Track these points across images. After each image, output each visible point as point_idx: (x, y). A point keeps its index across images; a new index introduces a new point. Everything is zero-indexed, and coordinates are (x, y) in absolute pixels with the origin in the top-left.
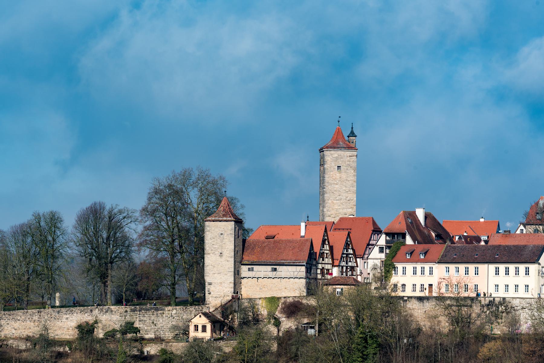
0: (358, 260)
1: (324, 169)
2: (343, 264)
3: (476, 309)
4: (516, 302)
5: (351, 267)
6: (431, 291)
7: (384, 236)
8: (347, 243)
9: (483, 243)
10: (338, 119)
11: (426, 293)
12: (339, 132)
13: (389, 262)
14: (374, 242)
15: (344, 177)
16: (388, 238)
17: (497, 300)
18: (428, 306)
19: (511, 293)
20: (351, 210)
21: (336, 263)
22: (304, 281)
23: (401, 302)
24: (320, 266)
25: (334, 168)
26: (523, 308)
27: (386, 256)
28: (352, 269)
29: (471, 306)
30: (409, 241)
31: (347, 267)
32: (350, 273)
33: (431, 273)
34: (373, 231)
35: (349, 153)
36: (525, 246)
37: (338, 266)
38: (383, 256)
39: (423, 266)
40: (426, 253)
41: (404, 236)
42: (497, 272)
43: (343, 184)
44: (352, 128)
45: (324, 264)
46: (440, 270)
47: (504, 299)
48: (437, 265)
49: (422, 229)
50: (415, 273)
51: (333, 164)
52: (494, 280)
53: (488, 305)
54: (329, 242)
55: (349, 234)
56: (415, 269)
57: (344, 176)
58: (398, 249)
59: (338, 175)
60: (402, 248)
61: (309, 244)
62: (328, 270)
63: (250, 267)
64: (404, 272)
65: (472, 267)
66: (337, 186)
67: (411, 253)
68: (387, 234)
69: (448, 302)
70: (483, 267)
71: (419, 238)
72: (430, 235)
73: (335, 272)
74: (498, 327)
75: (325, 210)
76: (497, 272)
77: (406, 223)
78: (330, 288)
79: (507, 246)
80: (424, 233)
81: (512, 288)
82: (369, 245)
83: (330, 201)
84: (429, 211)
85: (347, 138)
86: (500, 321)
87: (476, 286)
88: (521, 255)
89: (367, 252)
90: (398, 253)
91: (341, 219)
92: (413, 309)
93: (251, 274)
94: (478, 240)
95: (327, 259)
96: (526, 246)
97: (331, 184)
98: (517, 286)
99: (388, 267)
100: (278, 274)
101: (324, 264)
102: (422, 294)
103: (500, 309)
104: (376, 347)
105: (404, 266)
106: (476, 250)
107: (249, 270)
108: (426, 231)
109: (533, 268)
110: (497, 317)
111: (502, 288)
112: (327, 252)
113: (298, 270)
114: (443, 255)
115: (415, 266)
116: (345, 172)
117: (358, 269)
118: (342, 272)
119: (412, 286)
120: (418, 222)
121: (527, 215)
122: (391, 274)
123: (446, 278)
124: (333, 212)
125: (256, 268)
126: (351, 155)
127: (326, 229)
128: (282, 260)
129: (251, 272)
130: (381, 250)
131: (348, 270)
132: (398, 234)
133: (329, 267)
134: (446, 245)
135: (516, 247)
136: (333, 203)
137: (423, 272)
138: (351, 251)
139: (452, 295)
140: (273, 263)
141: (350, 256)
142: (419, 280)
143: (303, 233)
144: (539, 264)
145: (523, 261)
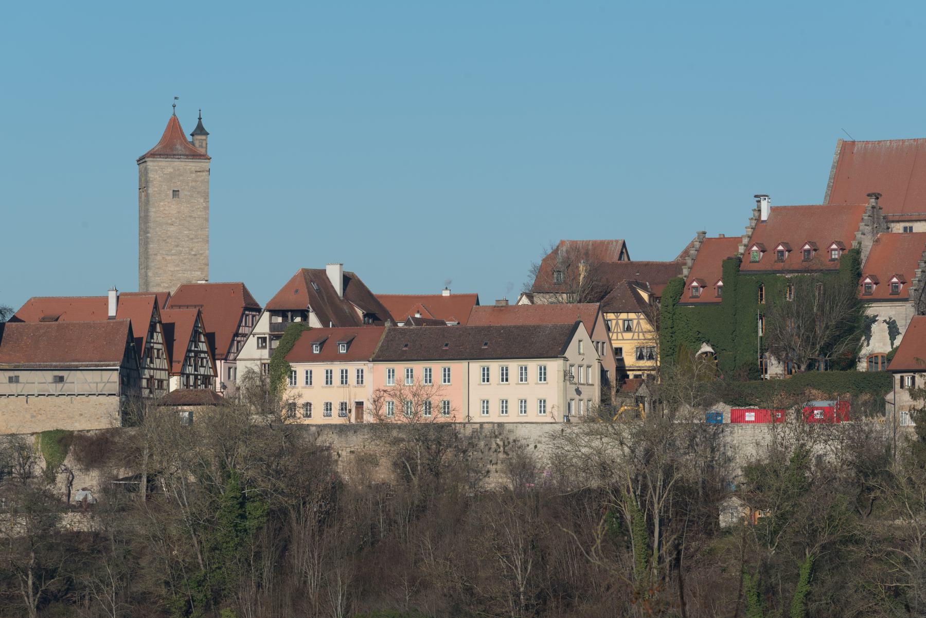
1: (147, 195)
2: (190, 370)
4: (522, 432)
5: (204, 376)
6: (360, 414)
7: (266, 315)
12: (174, 126)
19: (513, 415)
20: (199, 273)
21: (177, 367)
22: (115, 400)
24: (147, 374)
25: (167, 195)
28: (207, 380)
31: (196, 377)
34: (246, 309)
35: (193, 165)
36: (536, 328)
37: (182, 374)
40: (349, 344)
41: (304, 315)
42: (486, 378)
44: (200, 119)
45: (154, 369)
47: (501, 425)
48: (371, 365)
50: (329, 380)
52: (479, 392)
61: (126, 331)
62: (161, 381)
63: (12, 374)
64: (309, 381)
65: (438, 367)
66: (172, 229)
68: (274, 312)
69: (395, 433)
70: (458, 368)
73: (174, 383)
75: (150, 274)
76: (486, 378)
77: (309, 292)
79: (503, 328)
81: (514, 407)
82: (237, 338)
83: (159, 257)
84: (348, 269)
85: (190, 139)
87: (447, 404)
89: (234, 349)
93: (14, 388)
95: (158, 360)
96: (538, 327)
99: (278, 369)
100: (66, 387)
101: (154, 369)
107: (11, 380)
109: (554, 366)
111: (495, 407)
112: (159, 346)
113: (105, 380)
114: (382, 346)
117: (218, 380)
118: (187, 385)
119: (323, 407)
125: (23, 376)
126: (198, 169)
128: (74, 361)
129: (13, 385)
131: (199, 382)
137: (344, 380)
140: (55, 366)
141: (202, 355)
142: (337, 395)
143: (112, 312)
144: (566, 359)
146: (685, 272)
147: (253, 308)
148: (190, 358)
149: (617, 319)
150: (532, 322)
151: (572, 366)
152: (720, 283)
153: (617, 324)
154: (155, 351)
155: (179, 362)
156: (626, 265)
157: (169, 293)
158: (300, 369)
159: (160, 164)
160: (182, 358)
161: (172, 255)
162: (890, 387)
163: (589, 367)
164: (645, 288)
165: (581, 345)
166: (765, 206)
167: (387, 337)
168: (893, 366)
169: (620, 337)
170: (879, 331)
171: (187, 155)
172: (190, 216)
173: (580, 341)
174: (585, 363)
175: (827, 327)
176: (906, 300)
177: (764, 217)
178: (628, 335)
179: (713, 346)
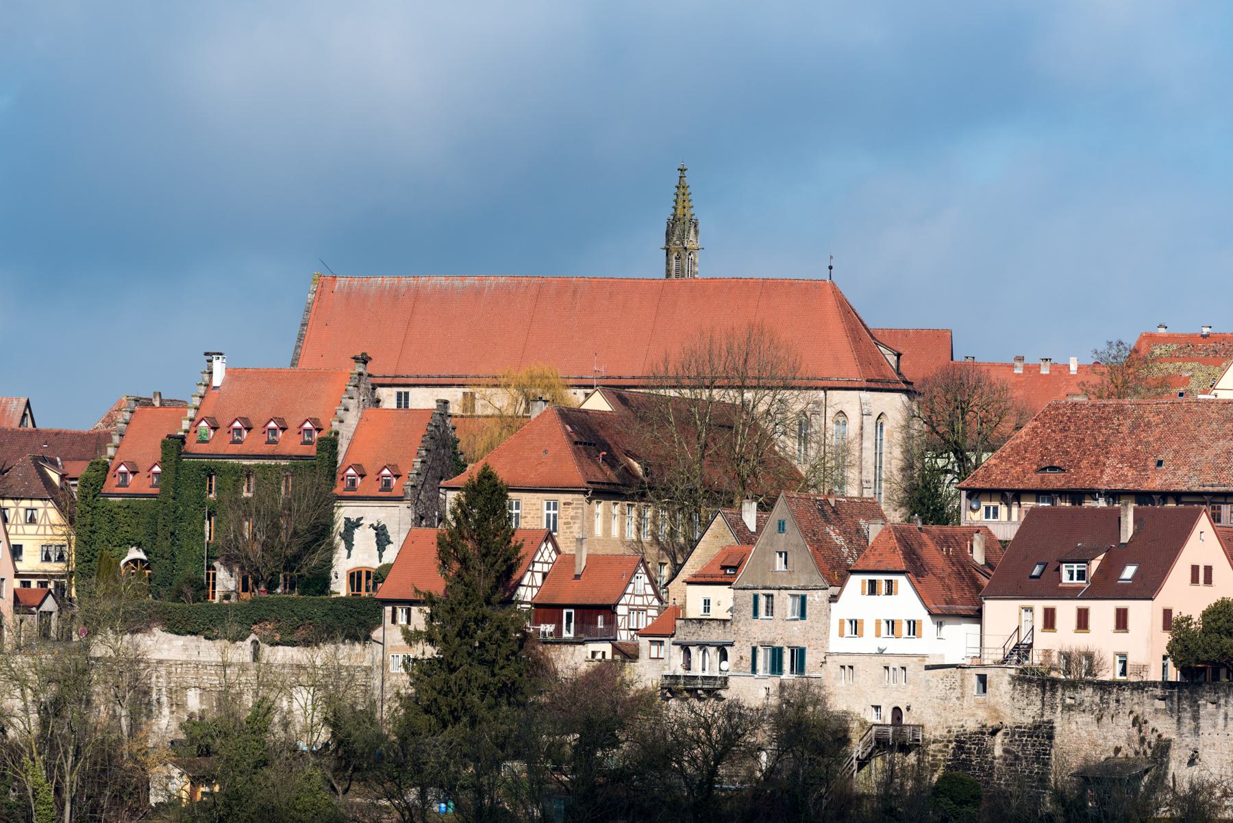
146: (111, 451)
149: (17, 507)
152: (157, 469)
153: (17, 513)
156: (30, 433)
162: (380, 623)
164: (54, 463)
166: (219, 367)
168: (384, 591)
170: (364, 537)
175: (295, 533)
176: (400, 499)
177: (217, 381)
178: (31, 529)
179: (146, 553)
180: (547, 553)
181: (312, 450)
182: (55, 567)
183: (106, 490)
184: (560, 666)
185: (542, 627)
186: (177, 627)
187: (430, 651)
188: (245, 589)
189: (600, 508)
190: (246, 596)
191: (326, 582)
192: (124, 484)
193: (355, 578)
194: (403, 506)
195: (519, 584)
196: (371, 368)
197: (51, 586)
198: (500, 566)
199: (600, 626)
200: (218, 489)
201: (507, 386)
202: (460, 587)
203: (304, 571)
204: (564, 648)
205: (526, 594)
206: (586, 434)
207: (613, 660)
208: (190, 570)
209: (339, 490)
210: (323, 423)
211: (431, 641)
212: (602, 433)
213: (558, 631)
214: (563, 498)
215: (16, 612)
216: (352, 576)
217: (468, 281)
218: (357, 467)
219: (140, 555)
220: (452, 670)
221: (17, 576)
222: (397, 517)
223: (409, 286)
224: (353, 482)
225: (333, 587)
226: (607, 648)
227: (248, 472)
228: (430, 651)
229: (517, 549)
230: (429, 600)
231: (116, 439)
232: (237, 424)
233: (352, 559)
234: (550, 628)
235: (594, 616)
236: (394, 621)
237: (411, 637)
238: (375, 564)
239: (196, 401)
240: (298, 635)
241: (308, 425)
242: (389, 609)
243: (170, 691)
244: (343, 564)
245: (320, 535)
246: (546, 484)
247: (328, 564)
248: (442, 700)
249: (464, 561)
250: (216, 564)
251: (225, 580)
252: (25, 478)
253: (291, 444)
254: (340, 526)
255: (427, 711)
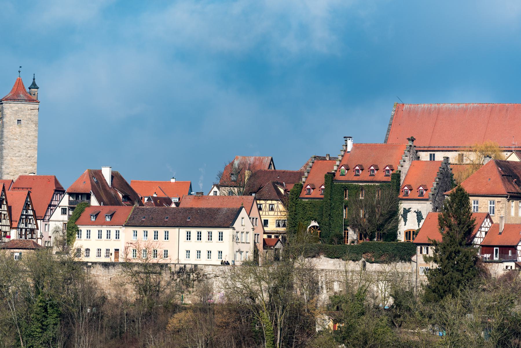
0: (39, 221)
3: (166, 276)
4: (208, 270)
5: (31, 229)
6: (117, 257)
7: (67, 196)
8: (27, 204)
9: (173, 206)
10: (19, 69)
11: (112, 259)
12: (19, 83)
13: (72, 225)
14: (56, 203)
15: (25, 131)
16: (71, 199)
17: (188, 267)
18: (114, 272)
19: (203, 260)
20: (31, 167)
21: (15, 225)
23: (85, 268)
25: (14, 122)
26: (216, 276)
27: (69, 218)
28: (32, 231)
29: (160, 273)
30: (94, 202)
32: (29, 236)
33: (117, 237)
34: (56, 191)
36: (218, 210)
37: (17, 228)
38: (65, 218)
39: (109, 229)
41: (88, 196)
42: (189, 237)
43: (23, 140)
44: (34, 79)
46: (127, 233)
47: (196, 266)
48: (124, 228)
49: (108, 189)
50: (100, 237)
51: (13, 118)
52: (185, 245)
53: (179, 272)
54: (7, 202)
55: (29, 194)
56: (100, 232)
57: (24, 130)
58: (82, 211)
59: (18, 129)
60: (87, 209)
62: (5, 232)
64: (88, 236)
65: (161, 231)
66: (17, 142)
67: (96, 215)
68: (70, 194)
69: (136, 269)
70: (173, 232)
71: (105, 199)
72: (117, 196)
73: (14, 234)
74: (189, 296)
76: (189, 237)
77: (92, 183)
78: (8, 252)
79: (200, 209)
80: (110, 193)
81: (204, 254)
83: (9, 158)
84: (115, 170)
85: (28, 90)
86: (191, 289)
87: (166, 252)
88: (215, 219)
89: (49, 214)
90: (83, 214)
91: (21, 178)
92: (98, 276)
94: (169, 202)
95: (4, 221)
96: (219, 209)
97: (10, 140)
98: (209, 252)
99: (71, 230)
102: (107, 260)
103: (192, 277)
104: (57, 317)
105: (88, 229)
106: (166, 213)
108: (112, 192)
109: (227, 233)
110: (188, 285)
111: (193, 254)
112: (5, 213)
114: (130, 218)
115: (100, 229)
116: (26, 127)
117: (39, 231)
119: (96, 251)
120: (104, 182)
121: (221, 176)
122: (74, 238)
123: (134, 242)
124: (12, 170)
127: (4, 187)
130: (64, 211)
131: (28, 233)
132: (82, 194)
133: (7, 229)
134: (133, 207)
135: (209, 210)
136: (12, 160)
137: (108, 236)
138: (30, 212)
139: (140, 261)
141: (30, 217)
142: (105, 244)
144: (234, 229)
145: (217, 225)
146: (304, 180)
147: (60, 191)
148: (23, 219)
149: (266, 204)
150: (216, 206)
151: (237, 232)
152: (323, 187)
153: (266, 206)
154: (3, 215)
155: (16, 221)
156: (272, 172)
157: (13, 181)
158: (84, 229)
159: (10, 104)
160: (18, 220)
161: (16, 157)
162: (415, 253)
163: (247, 233)
164: (282, 185)
165: (243, 222)
166: (350, 143)
167: (133, 212)
169: (267, 213)
170: (412, 217)
171: (26, 101)
172: (27, 135)
173: (243, 218)
174: (245, 231)
175: (381, 215)
176: (427, 200)
177: (349, 149)
178: (272, 213)
179: (319, 223)
180: (487, 223)
181: (389, 179)
182: (282, 229)
183: (301, 196)
184: (492, 272)
185: (485, 256)
186: (331, 255)
187: (435, 266)
188: (361, 239)
189: (513, 204)
190: (361, 242)
191: (395, 236)
192: (309, 193)
193: (408, 234)
194: (428, 203)
195: (475, 237)
196: (415, 143)
197: (280, 238)
198: (466, 229)
199: (510, 255)
200: (349, 195)
201: (475, 151)
202: (448, 238)
203: (385, 231)
204: (494, 264)
205: (478, 241)
206: (508, 171)
207: (515, 270)
208: (337, 231)
209: (401, 196)
210: (394, 167)
211: (436, 261)
212: (515, 171)
213: (492, 257)
214: (497, 199)
215: (264, 248)
216: (406, 233)
217: (461, 106)
218: (409, 186)
219: (316, 224)
220: (444, 274)
221: (265, 233)
222: (426, 208)
223: (435, 108)
224: (407, 193)
225: (398, 238)
226: (513, 264)
227: (362, 188)
228: (435, 266)
229: (473, 221)
230: (435, 244)
231: (306, 174)
232: (357, 168)
233: (407, 225)
234: (488, 256)
235: (507, 251)
236: (421, 253)
237: (427, 260)
238: (416, 228)
239: (340, 158)
240: (382, 259)
241: (387, 168)
242: (419, 247)
243: (327, 283)
244: (403, 228)
245: (393, 215)
246: (490, 193)
247: (396, 228)
248: (440, 287)
249: (450, 226)
250: (348, 228)
251: (352, 235)
252: (269, 191)
253: (380, 176)
254: (401, 211)
255: (434, 291)
